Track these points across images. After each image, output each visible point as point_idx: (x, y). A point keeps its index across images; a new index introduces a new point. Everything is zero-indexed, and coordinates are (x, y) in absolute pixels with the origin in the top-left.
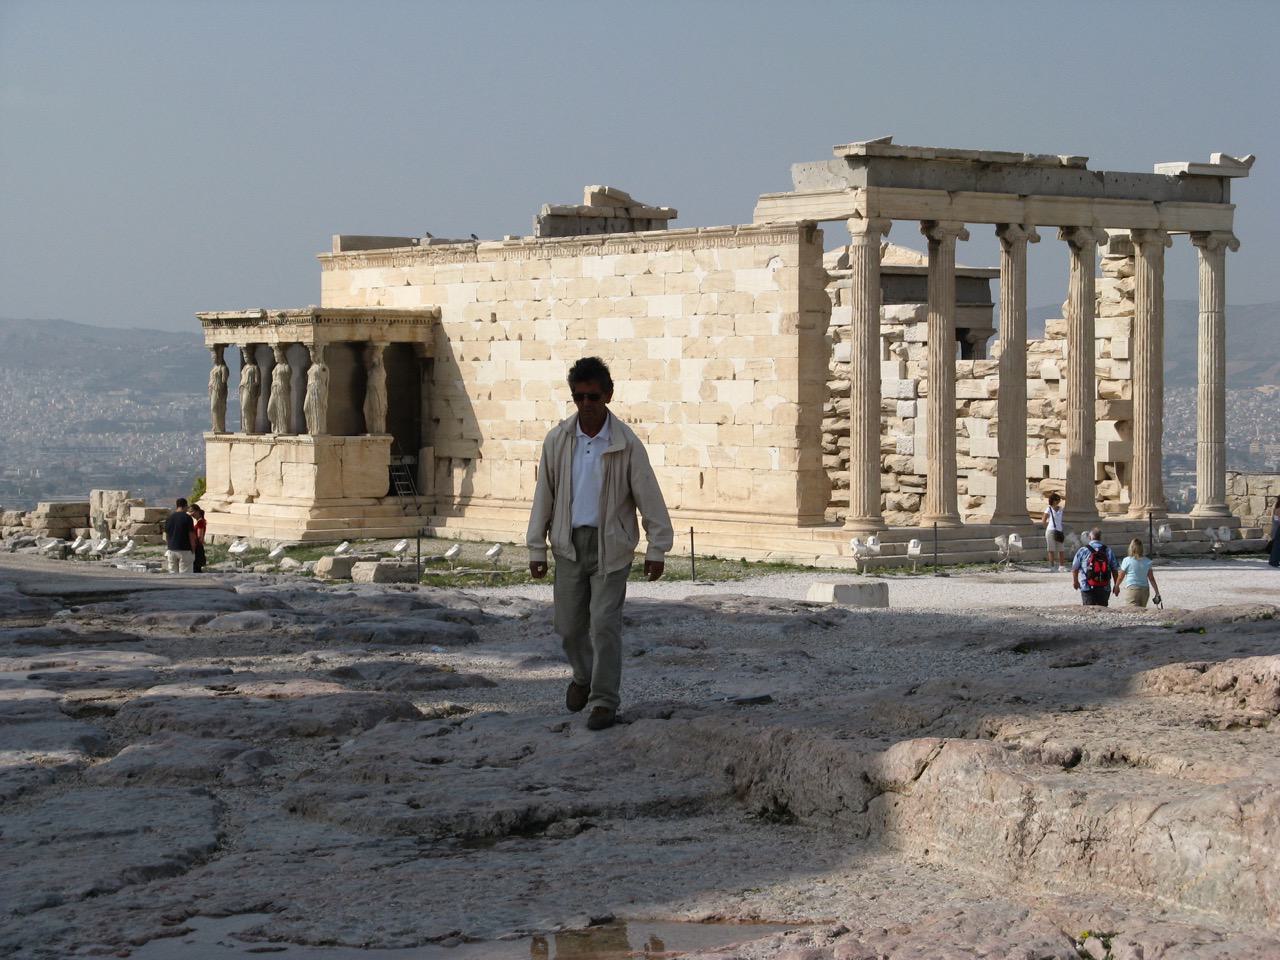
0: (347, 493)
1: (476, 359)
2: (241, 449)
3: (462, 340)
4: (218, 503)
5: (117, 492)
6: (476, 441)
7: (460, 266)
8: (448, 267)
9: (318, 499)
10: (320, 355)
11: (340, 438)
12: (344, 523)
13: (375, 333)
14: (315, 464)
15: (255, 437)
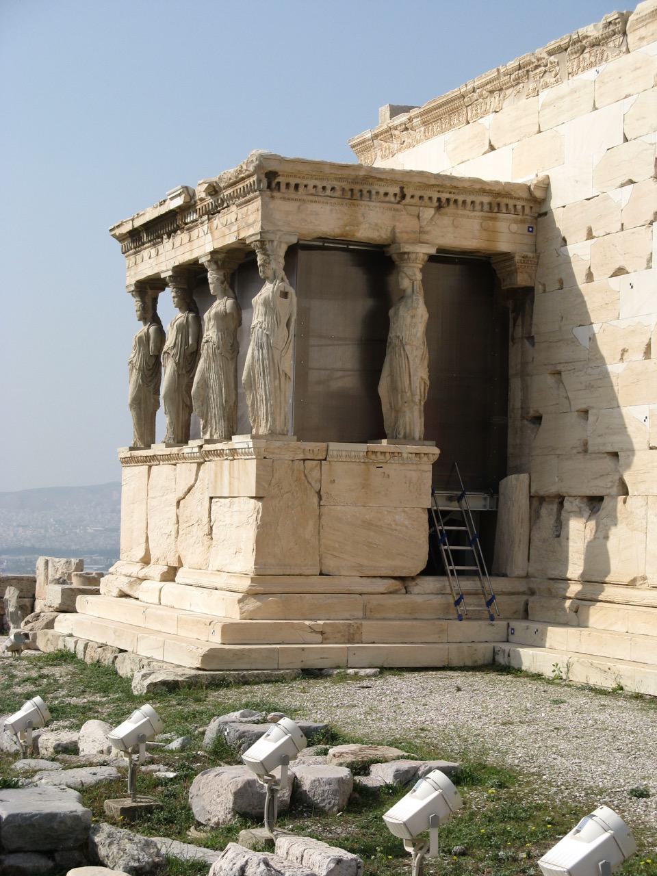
0: (330, 564)
1: (620, 271)
2: (162, 471)
3: (590, 236)
4: (126, 580)
5: (63, 560)
6: (615, 455)
7: (590, 74)
8: (565, 87)
9: (260, 575)
10: (278, 263)
11: (317, 446)
12: (312, 630)
13: (405, 224)
14: (258, 498)
15: (175, 450)
